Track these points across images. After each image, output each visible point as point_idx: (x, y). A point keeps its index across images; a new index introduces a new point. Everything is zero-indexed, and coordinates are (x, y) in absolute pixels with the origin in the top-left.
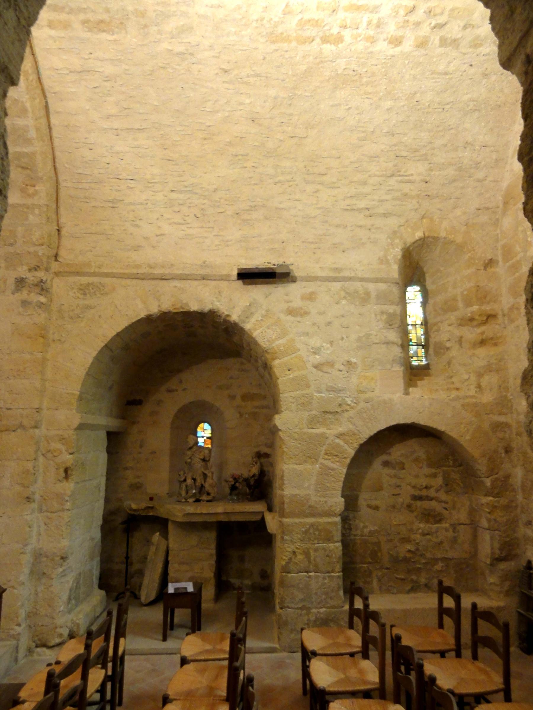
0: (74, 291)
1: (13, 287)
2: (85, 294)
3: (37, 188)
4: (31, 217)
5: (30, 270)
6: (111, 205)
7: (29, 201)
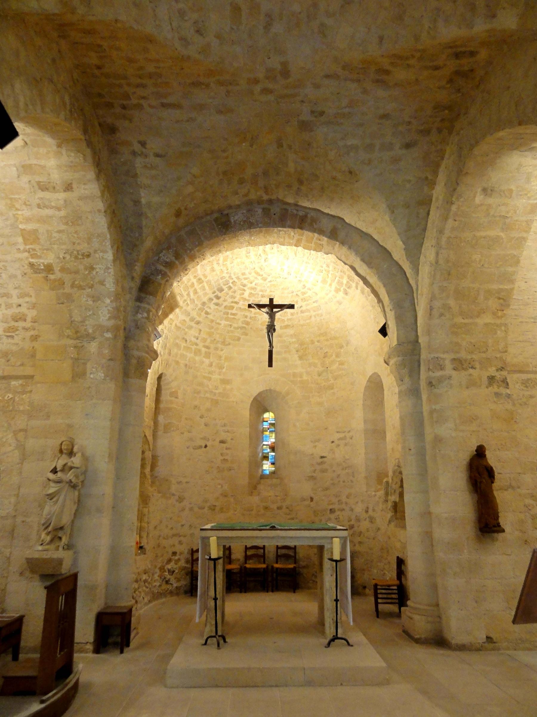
0: (518, 384)
1: (487, 383)
2: (526, 387)
3: (504, 312)
4: (499, 332)
5: (497, 370)
6: (533, 320)
7: (498, 321)
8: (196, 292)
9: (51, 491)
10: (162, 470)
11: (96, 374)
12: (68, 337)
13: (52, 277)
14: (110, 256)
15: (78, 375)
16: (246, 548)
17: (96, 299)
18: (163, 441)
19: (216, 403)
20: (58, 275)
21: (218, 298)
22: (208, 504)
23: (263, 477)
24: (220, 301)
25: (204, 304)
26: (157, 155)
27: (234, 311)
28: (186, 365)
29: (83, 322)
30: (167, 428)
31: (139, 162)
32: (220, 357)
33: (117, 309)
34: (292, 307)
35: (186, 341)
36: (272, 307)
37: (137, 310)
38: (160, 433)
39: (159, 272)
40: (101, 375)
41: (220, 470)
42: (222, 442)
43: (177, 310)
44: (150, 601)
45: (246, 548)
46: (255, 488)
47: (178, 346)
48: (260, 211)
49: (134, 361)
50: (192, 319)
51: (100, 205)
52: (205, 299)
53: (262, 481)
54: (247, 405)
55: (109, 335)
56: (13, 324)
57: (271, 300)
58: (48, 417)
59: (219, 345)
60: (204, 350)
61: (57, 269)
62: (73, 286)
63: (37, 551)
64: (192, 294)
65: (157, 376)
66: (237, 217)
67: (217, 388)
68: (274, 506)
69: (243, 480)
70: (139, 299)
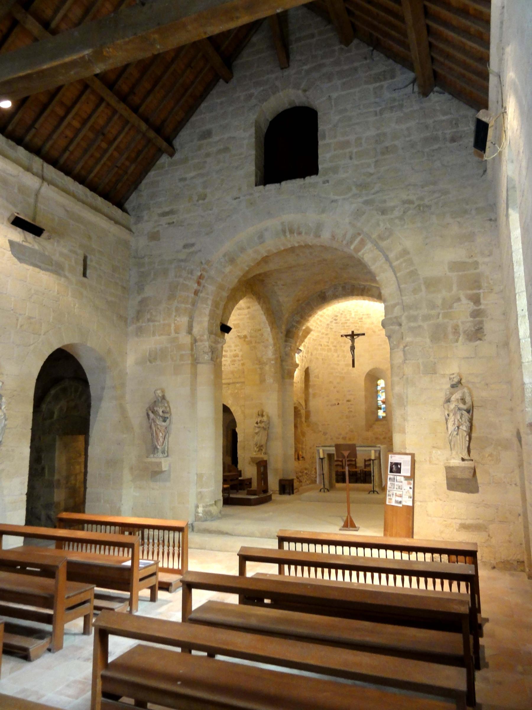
8: (321, 321)
9: (257, 431)
10: (313, 418)
11: (270, 380)
12: (257, 364)
13: (247, 340)
14: (269, 329)
15: (262, 381)
16: (365, 461)
17: (266, 347)
18: (314, 404)
19: (343, 378)
20: (249, 339)
21: (336, 320)
22: (341, 436)
23: (378, 419)
24: (338, 321)
25: (328, 325)
26: (283, 285)
27: (348, 324)
28: (323, 359)
29: (262, 357)
30: (314, 396)
31: (276, 288)
32: (344, 351)
33: (276, 350)
34: (364, 334)
35: (321, 345)
36: (353, 336)
37: (285, 346)
38: (311, 398)
39: (293, 326)
40: (272, 380)
41: (348, 417)
42: (348, 401)
43: (312, 333)
44: (310, 483)
45: (365, 461)
46: (371, 427)
47: (316, 349)
48: (340, 289)
49: (286, 371)
50: (323, 334)
51: (262, 312)
52: (328, 322)
53: (377, 423)
54: (363, 378)
55: (273, 362)
56: (234, 358)
57: (353, 332)
58: (252, 400)
59: (342, 344)
60: (333, 348)
61: (248, 336)
62: (256, 342)
63: (254, 455)
64: (319, 323)
65: (304, 370)
66: (329, 293)
67: (343, 369)
68: (381, 437)
69: (362, 422)
70: (286, 341)
